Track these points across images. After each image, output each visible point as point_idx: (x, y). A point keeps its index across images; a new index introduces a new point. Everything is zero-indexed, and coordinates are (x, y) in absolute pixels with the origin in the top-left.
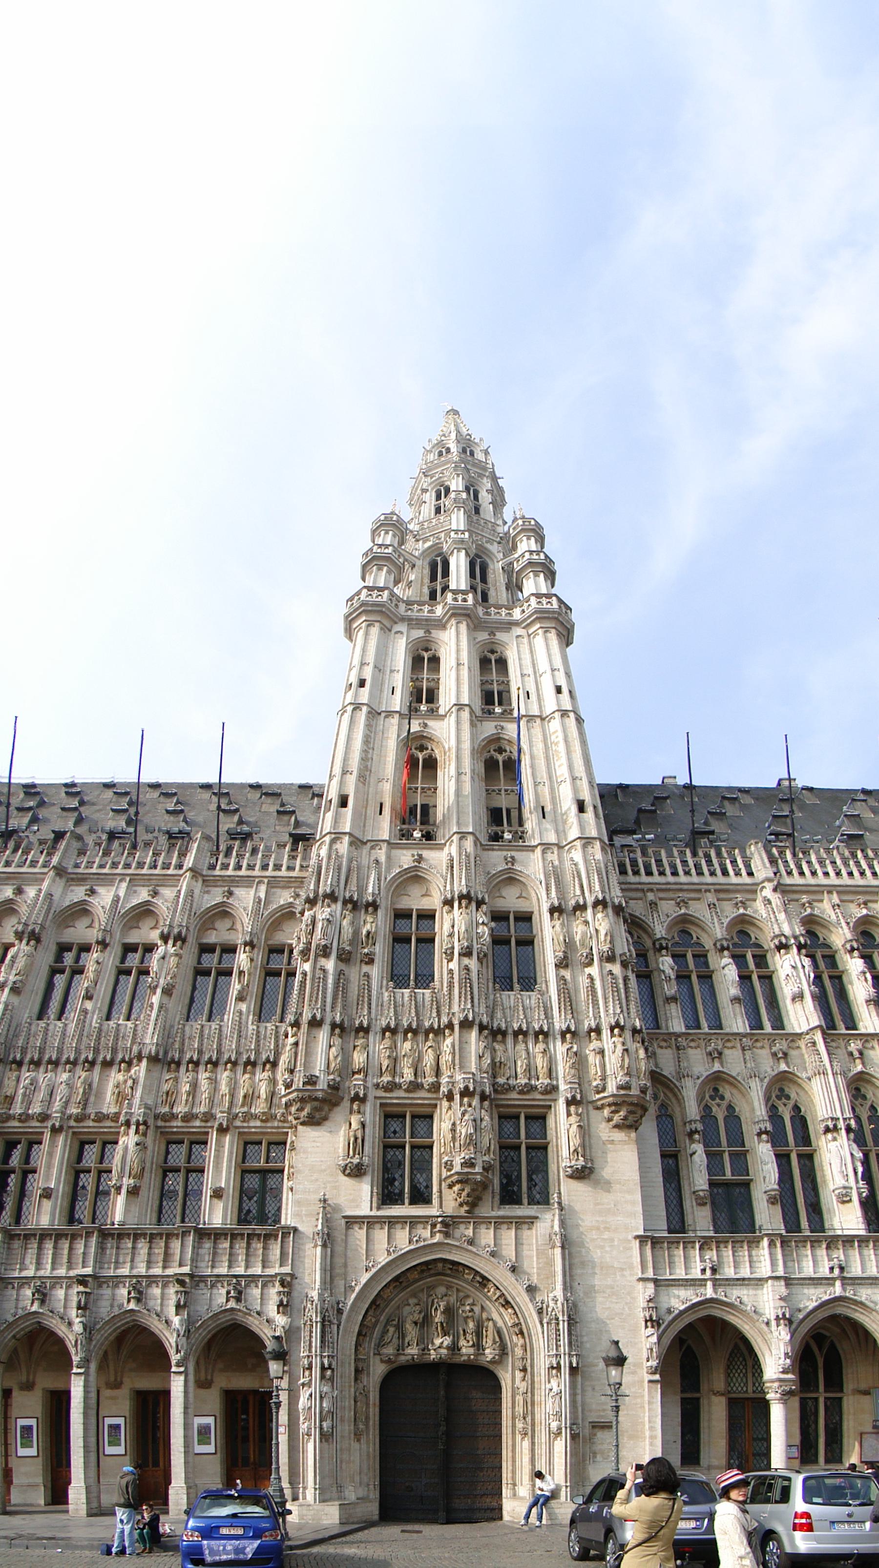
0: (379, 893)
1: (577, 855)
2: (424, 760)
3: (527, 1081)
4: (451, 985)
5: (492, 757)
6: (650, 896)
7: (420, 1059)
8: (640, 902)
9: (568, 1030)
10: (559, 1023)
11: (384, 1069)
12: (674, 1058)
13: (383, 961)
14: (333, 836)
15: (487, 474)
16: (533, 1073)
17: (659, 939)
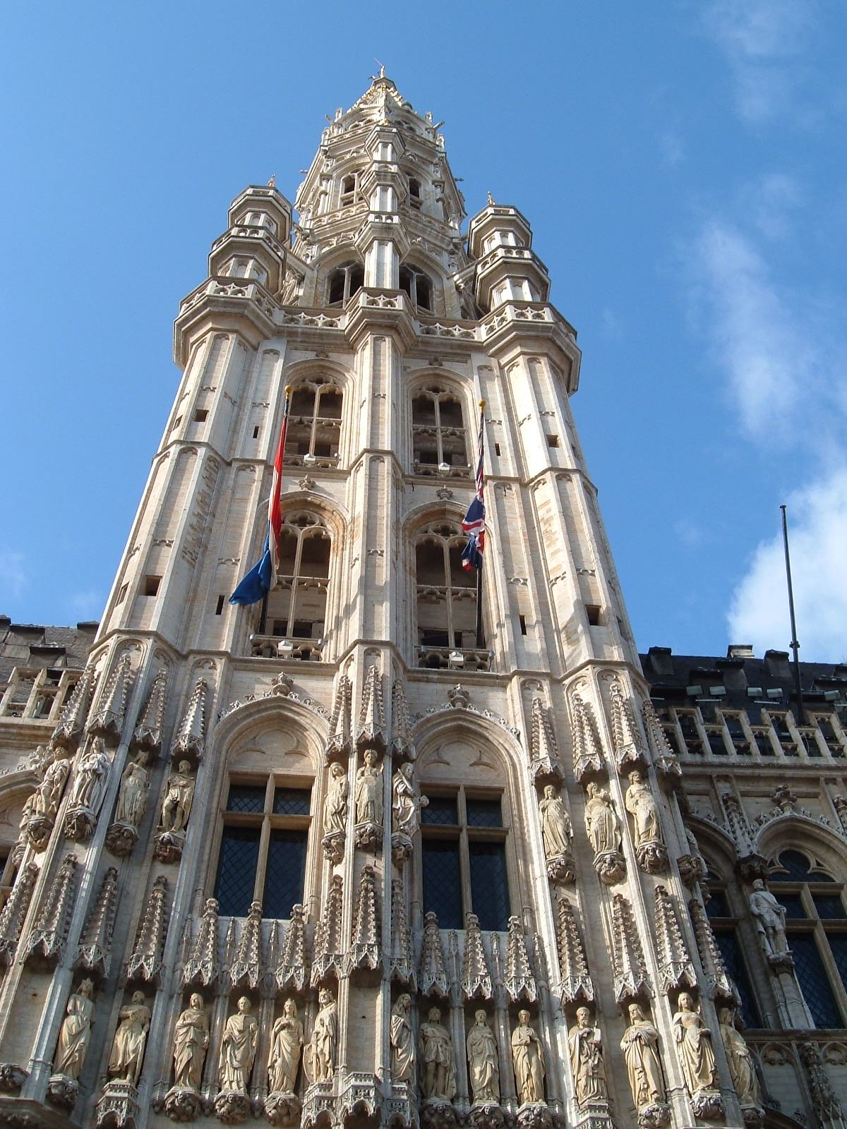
0: (205, 738)
1: (588, 692)
2: (306, 541)
3: (495, 1104)
4: (335, 904)
5: (430, 542)
6: (723, 788)
7: (261, 1052)
8: (704, 798)
9: (580, 999)
10: (561, 986)
11: (179, 1068)
12: (800, 1083)
13: (200, 861)
14: (124, 637)
15: (436, 160)
16: (509, 1089)
17: (745, 860)
